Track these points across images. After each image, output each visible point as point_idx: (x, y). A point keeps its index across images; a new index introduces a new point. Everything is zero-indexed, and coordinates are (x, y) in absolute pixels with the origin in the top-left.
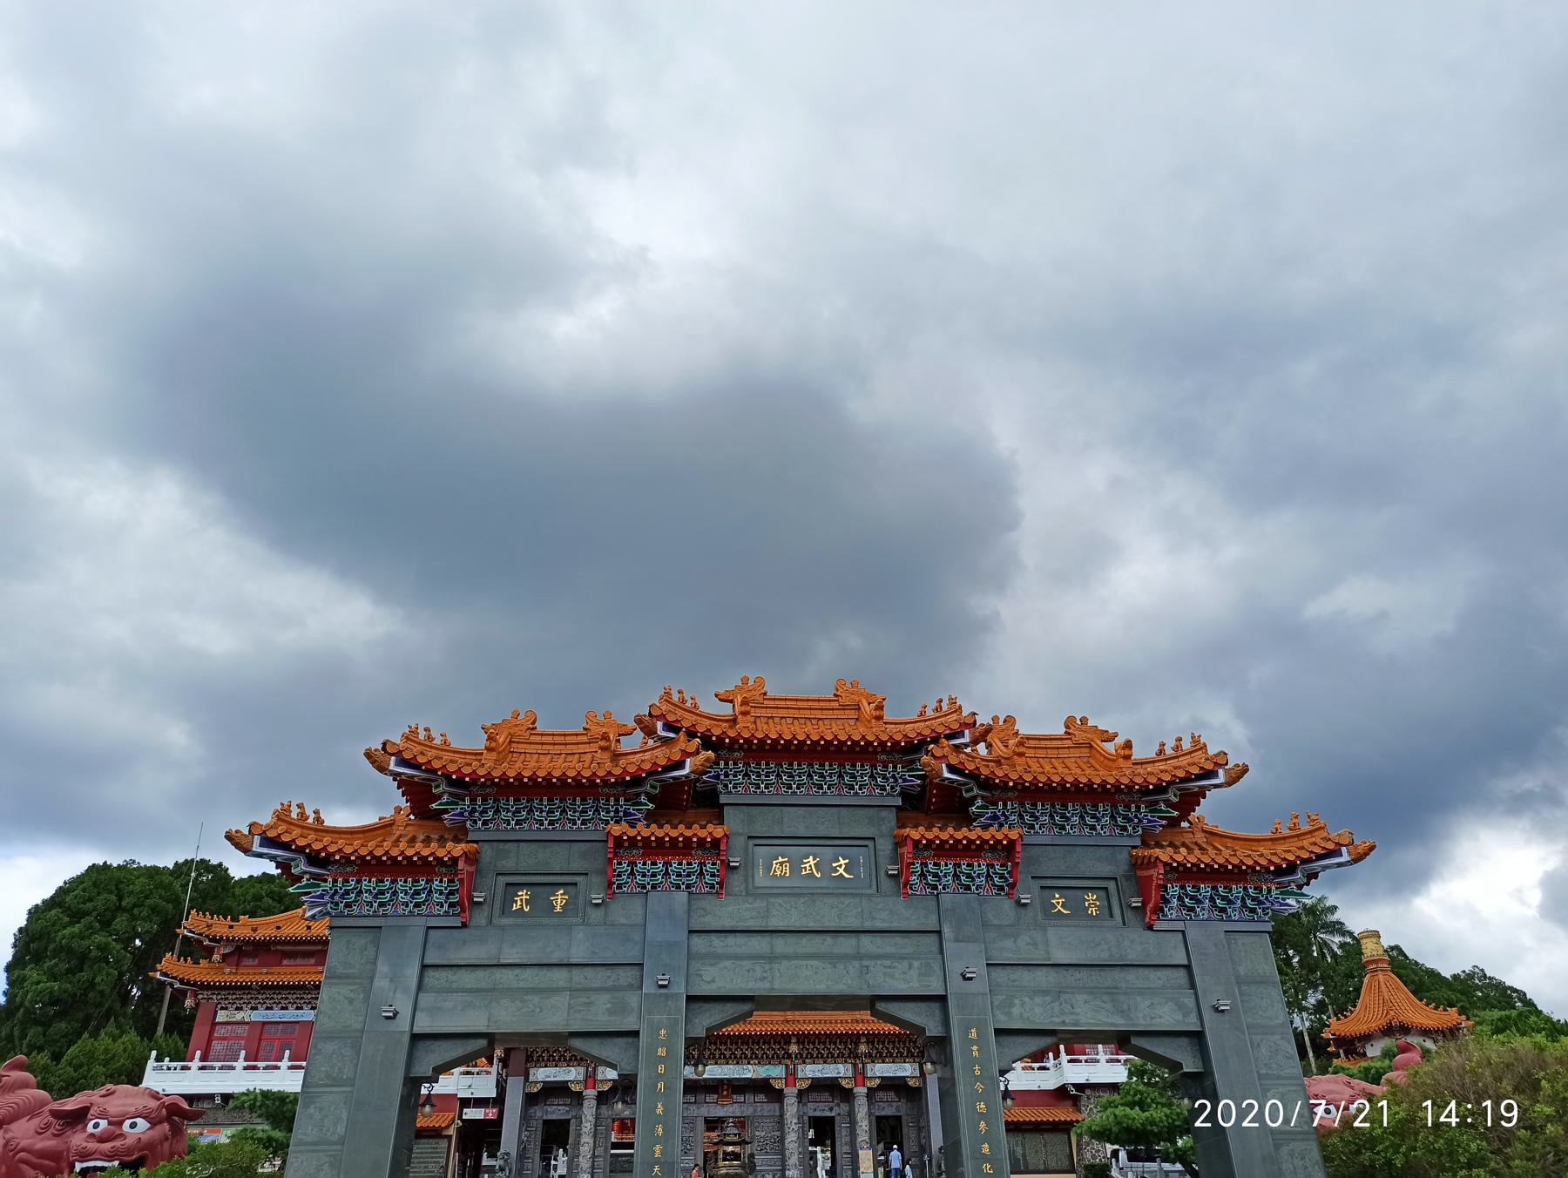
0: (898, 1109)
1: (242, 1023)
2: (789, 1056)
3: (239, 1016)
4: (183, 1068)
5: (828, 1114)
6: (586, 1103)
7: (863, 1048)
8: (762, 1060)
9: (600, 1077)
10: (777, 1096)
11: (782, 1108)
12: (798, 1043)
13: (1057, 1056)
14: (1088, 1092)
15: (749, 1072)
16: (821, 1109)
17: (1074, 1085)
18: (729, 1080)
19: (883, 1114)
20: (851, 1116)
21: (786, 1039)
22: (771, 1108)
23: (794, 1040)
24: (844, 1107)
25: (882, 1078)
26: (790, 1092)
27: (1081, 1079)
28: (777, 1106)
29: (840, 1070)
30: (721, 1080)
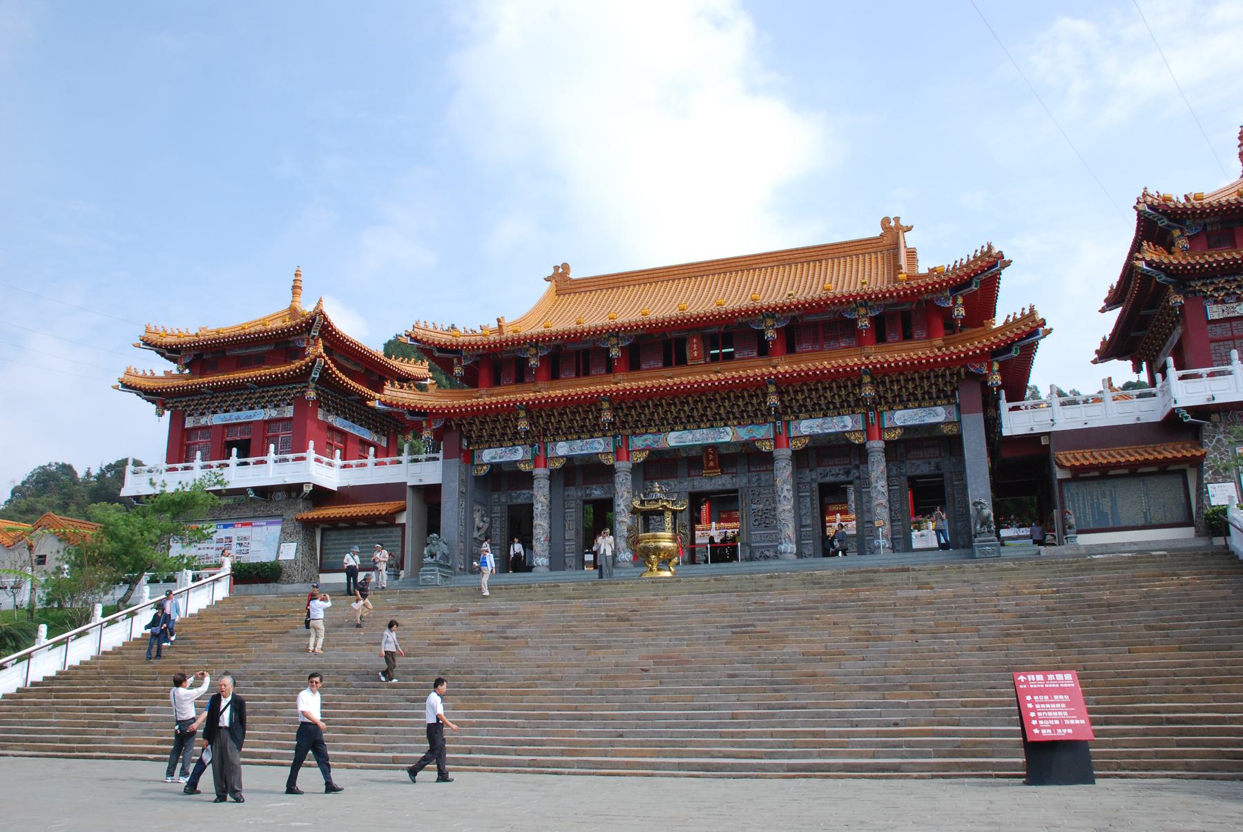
0: (938, 467)
1: (206, 428)
3: (203, 421)
4: (186, 468)
8: (741, 419)
10: (768, 460)
13: (1164, 376)
14: (1215, 417)
15: (727, 435)
17: (1189, 409)
18: (714, 447)
19: (918, 472)
20: (864, 483)
25: (905, 428)
27: (1199, 400)
30: (705, 447)
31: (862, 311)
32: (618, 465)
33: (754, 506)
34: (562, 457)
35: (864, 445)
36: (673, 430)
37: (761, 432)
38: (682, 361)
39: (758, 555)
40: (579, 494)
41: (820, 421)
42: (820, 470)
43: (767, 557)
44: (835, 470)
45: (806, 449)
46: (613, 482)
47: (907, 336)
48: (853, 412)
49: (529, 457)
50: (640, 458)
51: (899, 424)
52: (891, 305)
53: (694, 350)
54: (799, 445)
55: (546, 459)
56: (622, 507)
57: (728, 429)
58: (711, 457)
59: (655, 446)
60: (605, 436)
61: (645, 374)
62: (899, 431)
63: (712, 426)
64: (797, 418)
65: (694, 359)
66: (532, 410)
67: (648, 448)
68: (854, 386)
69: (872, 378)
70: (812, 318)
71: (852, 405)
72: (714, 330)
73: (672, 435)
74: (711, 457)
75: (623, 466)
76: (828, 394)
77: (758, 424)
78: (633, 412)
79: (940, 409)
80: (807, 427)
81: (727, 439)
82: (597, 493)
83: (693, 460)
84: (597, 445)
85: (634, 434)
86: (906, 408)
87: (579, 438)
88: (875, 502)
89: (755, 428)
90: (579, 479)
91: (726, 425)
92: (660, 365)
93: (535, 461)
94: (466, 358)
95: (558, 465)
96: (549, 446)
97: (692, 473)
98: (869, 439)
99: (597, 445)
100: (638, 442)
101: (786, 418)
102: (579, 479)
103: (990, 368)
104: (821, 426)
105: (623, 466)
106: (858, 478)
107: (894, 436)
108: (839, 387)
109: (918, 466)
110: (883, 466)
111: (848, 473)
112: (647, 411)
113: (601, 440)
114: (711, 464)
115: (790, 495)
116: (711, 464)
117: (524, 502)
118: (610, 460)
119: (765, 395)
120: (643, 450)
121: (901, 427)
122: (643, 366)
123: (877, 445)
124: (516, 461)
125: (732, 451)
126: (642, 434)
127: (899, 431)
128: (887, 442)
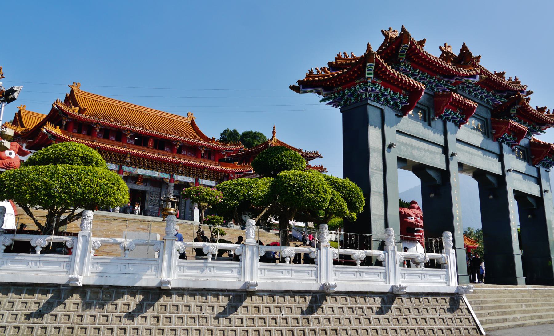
12: (182, 167)
15: (156, 174)
18: (142, 175)
28: (159, 189)
37: (167, 176)
41: (183, 177)
43: (153, 216)
45: (178, 184)
47: (209, 158)
50: (127, 175)
54: (176, 183)
67: (130, 172)
73: (139, 170)
79: (214, 182)
80: (180, 178)
81: (156, 176)
94: (68, 118)
103: (234, 176)
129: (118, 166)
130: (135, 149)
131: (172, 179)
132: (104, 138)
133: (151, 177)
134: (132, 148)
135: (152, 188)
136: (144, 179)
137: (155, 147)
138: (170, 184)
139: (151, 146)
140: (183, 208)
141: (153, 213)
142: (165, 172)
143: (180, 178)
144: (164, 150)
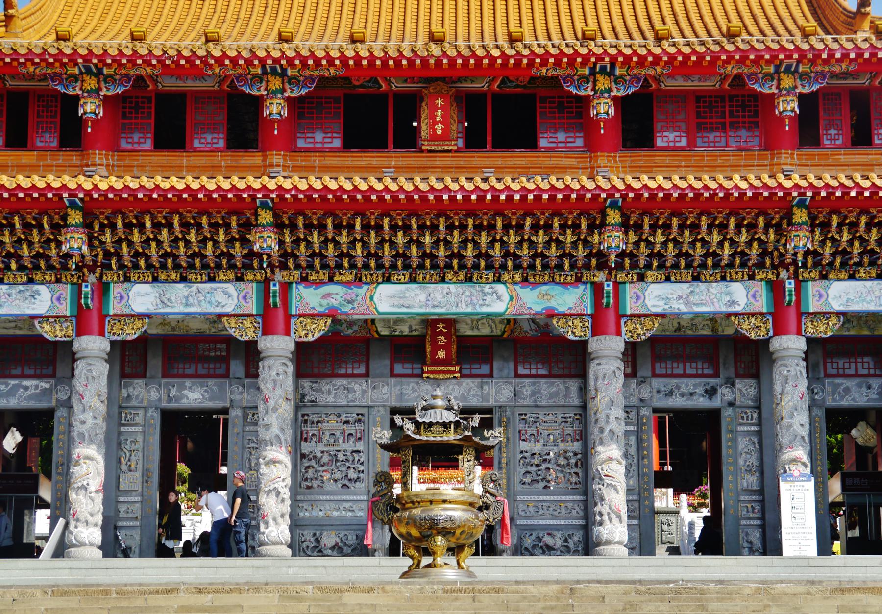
2: (602, 256)
5: (702, 402)
6: (80, 367)
7: (801, 240)
9: (114, 307)
11: (583, 390)
12: (625, 226)
15: (495, 300)
16: (687, 393)
18: (450, 323)
19: (846, 402)
20: (763, 411)
21: (591, 211)
22: (555, 391)
23: (614, 217)
24: (745, 389)
25: (846, 316)
26: (608, 350)
28: (574, 385)
29: (736, 298)
31: (787, 82)
32: (266, 343)
33: (523, 446)
34: (141, 316)
35: (766, 342)
36: (388, 280)
37: (568, 299)
38: (408, 140)
39: (528, 542)
40: (154, 395)
41: (683, 288)
42: (657, 383)
43: (548, 550)
44: (688, 385)
46: (582, 375)
48: (752, 277)
49: (66, 309)
50: (315, 331)
51: (837, 307)
52: (845, 75)
53: (436, 119)
54: (642, 332)
55: (102, 318)
56: (275, 430)
57: (500, 288)
58: (442, 340)
59: (347, 309)
60: (240, 279)
61: (545, 161)
62: (834, 320)
63: (469, 280)
64: (641, 278)
65: (434, 138)
66: (97, 210)
67: (332, 314)
68: (591, 228)
69: (812, 218)
70: (679, 83)
71: (767, 263)
72: (480, 85)
74: (442, 340)
75: (278, 347)
76: (400, 238)
77: (565, 284)
78: (326, 234)
80: (660, 298)
81: (498, 307)
82: (194, 395)
83: (414, 347)
84: (222, 299)
85: (304, 280)
86: (852, 277)
87: (183, 279)
88: (788, 455)
89: (555, 290)
90: (155, 363)
91: (499, 280)
92: (337, 143)
93: (83, 320)
95: (131, 333)
96: (115, 291)
97: (398, 369)
98: (779, 330)
99: (222, 299)
100: (309, 298)
101: (621, 277)
102: (155, 363)
104: (686, 300)
105: (278, 347)
106: (731, 404)
107: (824, 330)
108: (450, 228)
109: (847, 390)
110: (803, 384)
111: (711, 392)
112: (221, 237)
113: (230, 288)
114: (441, 354)
115: (620, 428)
116: (441, 354)
117: (33, 404)
118: (246, 331)
119: (247, 226)
120: (321, 315)
121: (838, 314)
122: (543, 143)
123: (790, 346)
124: (33, 317)
125: (485, 331)
126: (319, 284)
127: (834, 320)
128: (810, 341)
129: (252, 290)
130: (349, 171)
131: (783, 313)
132: (160, 145)
133: (430, 323)
134: (334, 171)
135: (527, 387)
136: (463, 340)
137: (474, 141)
138: (595, 345)
139: (445, 137)
140: (751, 481)
141: (550, 530)
142: (552, 270)
143: (660, 298)
144: (531, 144)
